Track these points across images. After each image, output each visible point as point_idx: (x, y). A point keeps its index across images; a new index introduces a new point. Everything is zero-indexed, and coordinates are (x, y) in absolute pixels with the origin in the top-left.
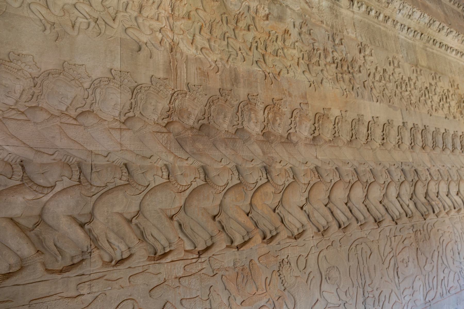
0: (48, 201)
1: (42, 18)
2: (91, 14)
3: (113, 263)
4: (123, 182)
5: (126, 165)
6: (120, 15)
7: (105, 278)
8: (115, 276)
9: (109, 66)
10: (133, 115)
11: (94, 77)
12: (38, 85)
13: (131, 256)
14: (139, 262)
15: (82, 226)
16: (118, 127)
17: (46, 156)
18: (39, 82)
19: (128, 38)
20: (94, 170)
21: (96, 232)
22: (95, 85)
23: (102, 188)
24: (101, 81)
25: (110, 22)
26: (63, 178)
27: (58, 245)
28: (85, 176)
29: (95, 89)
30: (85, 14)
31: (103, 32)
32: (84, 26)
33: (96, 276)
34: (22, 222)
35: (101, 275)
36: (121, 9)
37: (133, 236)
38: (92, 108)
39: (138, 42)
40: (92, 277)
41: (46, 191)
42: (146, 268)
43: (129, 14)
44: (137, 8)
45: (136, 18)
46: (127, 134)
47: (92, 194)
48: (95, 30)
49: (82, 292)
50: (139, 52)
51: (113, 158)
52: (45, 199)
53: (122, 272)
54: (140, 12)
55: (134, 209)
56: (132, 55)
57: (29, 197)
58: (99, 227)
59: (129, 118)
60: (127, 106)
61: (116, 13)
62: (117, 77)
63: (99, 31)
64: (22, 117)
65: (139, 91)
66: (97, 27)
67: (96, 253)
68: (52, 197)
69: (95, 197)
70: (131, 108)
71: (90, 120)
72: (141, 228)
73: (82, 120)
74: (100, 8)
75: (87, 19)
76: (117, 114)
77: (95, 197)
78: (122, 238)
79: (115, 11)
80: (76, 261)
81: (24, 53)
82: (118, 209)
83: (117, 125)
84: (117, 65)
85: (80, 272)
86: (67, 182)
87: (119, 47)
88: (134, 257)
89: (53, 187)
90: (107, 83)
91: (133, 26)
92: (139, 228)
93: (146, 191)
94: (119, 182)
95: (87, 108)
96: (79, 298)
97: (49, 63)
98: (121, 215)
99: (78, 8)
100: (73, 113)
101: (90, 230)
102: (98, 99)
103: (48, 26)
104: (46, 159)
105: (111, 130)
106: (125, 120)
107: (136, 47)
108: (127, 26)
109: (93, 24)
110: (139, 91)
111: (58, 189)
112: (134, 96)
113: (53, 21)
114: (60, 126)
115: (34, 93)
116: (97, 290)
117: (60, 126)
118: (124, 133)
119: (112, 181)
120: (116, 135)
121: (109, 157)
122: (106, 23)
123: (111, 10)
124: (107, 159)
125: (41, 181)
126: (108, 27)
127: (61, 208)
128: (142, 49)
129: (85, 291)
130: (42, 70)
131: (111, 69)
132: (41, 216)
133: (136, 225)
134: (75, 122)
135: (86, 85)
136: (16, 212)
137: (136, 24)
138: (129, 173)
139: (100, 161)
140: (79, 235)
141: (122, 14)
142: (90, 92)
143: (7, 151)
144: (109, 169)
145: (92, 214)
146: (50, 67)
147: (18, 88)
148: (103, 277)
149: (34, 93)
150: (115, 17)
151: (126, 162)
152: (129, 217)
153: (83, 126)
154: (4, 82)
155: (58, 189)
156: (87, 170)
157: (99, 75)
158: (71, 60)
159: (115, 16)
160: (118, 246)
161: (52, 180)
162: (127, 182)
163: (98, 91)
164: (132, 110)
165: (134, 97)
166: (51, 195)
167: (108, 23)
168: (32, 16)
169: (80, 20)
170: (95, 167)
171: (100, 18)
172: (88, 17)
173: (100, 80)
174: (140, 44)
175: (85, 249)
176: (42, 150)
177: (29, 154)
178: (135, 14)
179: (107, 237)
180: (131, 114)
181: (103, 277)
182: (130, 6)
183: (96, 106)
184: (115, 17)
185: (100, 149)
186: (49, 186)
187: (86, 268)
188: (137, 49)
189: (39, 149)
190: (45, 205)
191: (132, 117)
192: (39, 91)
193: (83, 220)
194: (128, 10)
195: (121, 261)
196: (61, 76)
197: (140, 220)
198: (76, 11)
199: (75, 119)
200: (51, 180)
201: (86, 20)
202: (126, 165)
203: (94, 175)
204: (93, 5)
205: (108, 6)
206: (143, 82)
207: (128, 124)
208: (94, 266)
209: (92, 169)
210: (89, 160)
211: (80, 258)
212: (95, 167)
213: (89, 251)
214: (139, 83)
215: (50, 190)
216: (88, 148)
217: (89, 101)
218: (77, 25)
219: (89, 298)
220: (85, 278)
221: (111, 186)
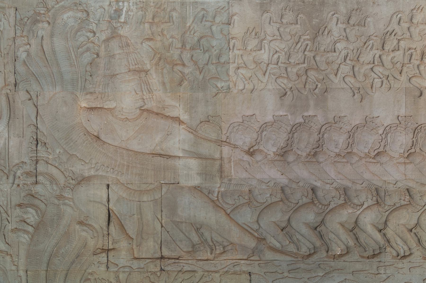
0: (359, 214)
1: (352, 86)
2: (384, 73)
3: (399, 257)
4: (406, 203)
5: (408, 190)
6: (405, 69)
7: (394, 266)
8: (400, 265)
9: (396, 114)
10: (414, 151)
11: (386, 125)
12: (351, 137)
13: (411, 254)
14: (416, 259)
15: (380, 231)
16: (403, 162)
17: (358, 185)
18: (352, 134)
19: (412, 86)
20: (387, 194)
21: (388, 236)
22: (387, 131)
23: (392, 207)
24: (391, 127)
25: (398, 77)
26: (368, 199)
27: (366, 241)
28: (380, 198)
29: (387, 134)
30: (380, 75)
31: (392, 86)
32: (379, 84)
33: (388, 264)
34: (347, 226)
35: (391, 263)
36: (406, 61)
37: (412, 241)
38: (385, 149)
39: (420, 88)
40: (386, 264)
41: (358, 208)
42: (421, 264)
43: (413, 64)
44: (419, 58)
45: (418, 66)
46: (410, 167)
47: (385, 211)
48: (387, 86)
49: (380, 272)
50: (421, 97)
51: (399, 185)
52: (359, 212)
53: (405, 264)
54: (422, 59)
55: (414, 222)
56: (414, 101)
57: (350, 211)
58: (390, 233)
59: (410, 153)
60: (410, 144)
61: (402, 67)
62: (403, 122)
63: (389, 86)
64: (344, 160)
65: (419, 131)
66: (388, 83)
67: (388, 249)
68: (362, 212)
69: (387, 213)
70: (413, 146)
71: (384, 159)
72: (418, 236)
73: (378, 159)
74: (390, 66)
75: (381, 78)
76: (402, 151)
77: (387, 213)
78: (405, 242)
79: (401, 65)
80: (376, 253)
81: (342, 115)
82: (402, 221)
83: (402, 160)
84: (403, 112)
85: (379, 260)
86: (370, 202)
87: (404, 96)
88: (412, 257)
89: (362, 205)
90: (395, 128)
91: (416, 75)
92: (417, 236)
93: (423, 210)
94: (403, 203)
95: (381, 149)
96: (379, 275)
97: (357, 120)
98: (404, 225)
99: (375, 71)
100: (373, 154)
101: (385, 235)
102: (389, 142)
103: (356, 92)
104: (359, 187)
105: (398, 164)
106: (408, 155)
107: (418, 93)
108: (410, 76)
109: (385, 82)
110: (419, 131)
111: (364, 207)
112: (415, 135)
113: (358, 87)
114: (365, 165)
115: (349, 142)
116: (389, 272)
117: (365, 165)
118: (407, 166)
119: (399, 201)
120: (402, 168)
121: (396, 185)
122: (394, 77)
123: (399, 66)
124: (395, 186)
125: (356, 201)
126: (396, 80)
127: (369, 219)
128: (423, 94)
129: (382, 272)
130: (353, 126)
131: (398, 116)
132: (356, 222)
133: (415, 233)
134: (373, 161)
135: (381, 132)
136: (344, 219)
137: (418, 72)
138: (410, 196)
139: (391, 187)
140: (378, 236)
141: (407, 65)
142: (384, 137)
143: (338, 182)
144: (397, 193)
145: (386, 223)
146: (358, 122)
147: (341, 141)
148: (393, 265)
149: (349, 142)
150: (402, 70)
151: (408, 188)
152: (410, 228)
153: (379, 163)
154: (334, 138)
155: (364, 207)
156: (382, 194)
157: (389, 123)
158: (370, 114)
159: (401, 69)
160: (402, 247)
161: (362, 201)
162: (409, 203)
163: (389, 135)
164: (413, 147)
165: (415, 136)
166: (361, 210)
167: (396, 77)
168: (345, 86)
169: (376, 80)
170: (387, 192)
171: (390, 75)
172: (382, 77)
173: (390, 126)
174: (422, 89)
175: (382, 246)
176: (356, 181)
177: (349, 184)
178: (418, 62)
179: (395, 240)
180: (413, 150)
181: (393, 265)
182: (413, 57)
183: (388, 147)
184: (402, 70)
185: (390, 179)
186: (360, 204)
187: (382, 257)
188: (419, 94)
189: (354, 181)
190: (358, 216)
191: (414, 152)
192: (352, 141)
193: (381, 227)
194: (411, 61)
195: (404, 257)
196: (365, 128)
197: (418, 229)
198: (373, 74)
199: (374, 158)
200: (361, 201)
201: (380, 80)
202: (408, 190)
203: (387, 198)
204: (385, 65)
205: (396, 62)
206: (422, 123)
207: (411, 158)
208: (388, 257)
209: (385, 193)
210: (384, 186)
211: (379, 251)
212: (387, 192)
213: (384, 247)
214: (419, 124)
215: (361, 207)
216: (383, 179)
217: (382, 144)
218: (374, 85)
219: (384, 276)
220: (382, 264)
221: (398, 205)
